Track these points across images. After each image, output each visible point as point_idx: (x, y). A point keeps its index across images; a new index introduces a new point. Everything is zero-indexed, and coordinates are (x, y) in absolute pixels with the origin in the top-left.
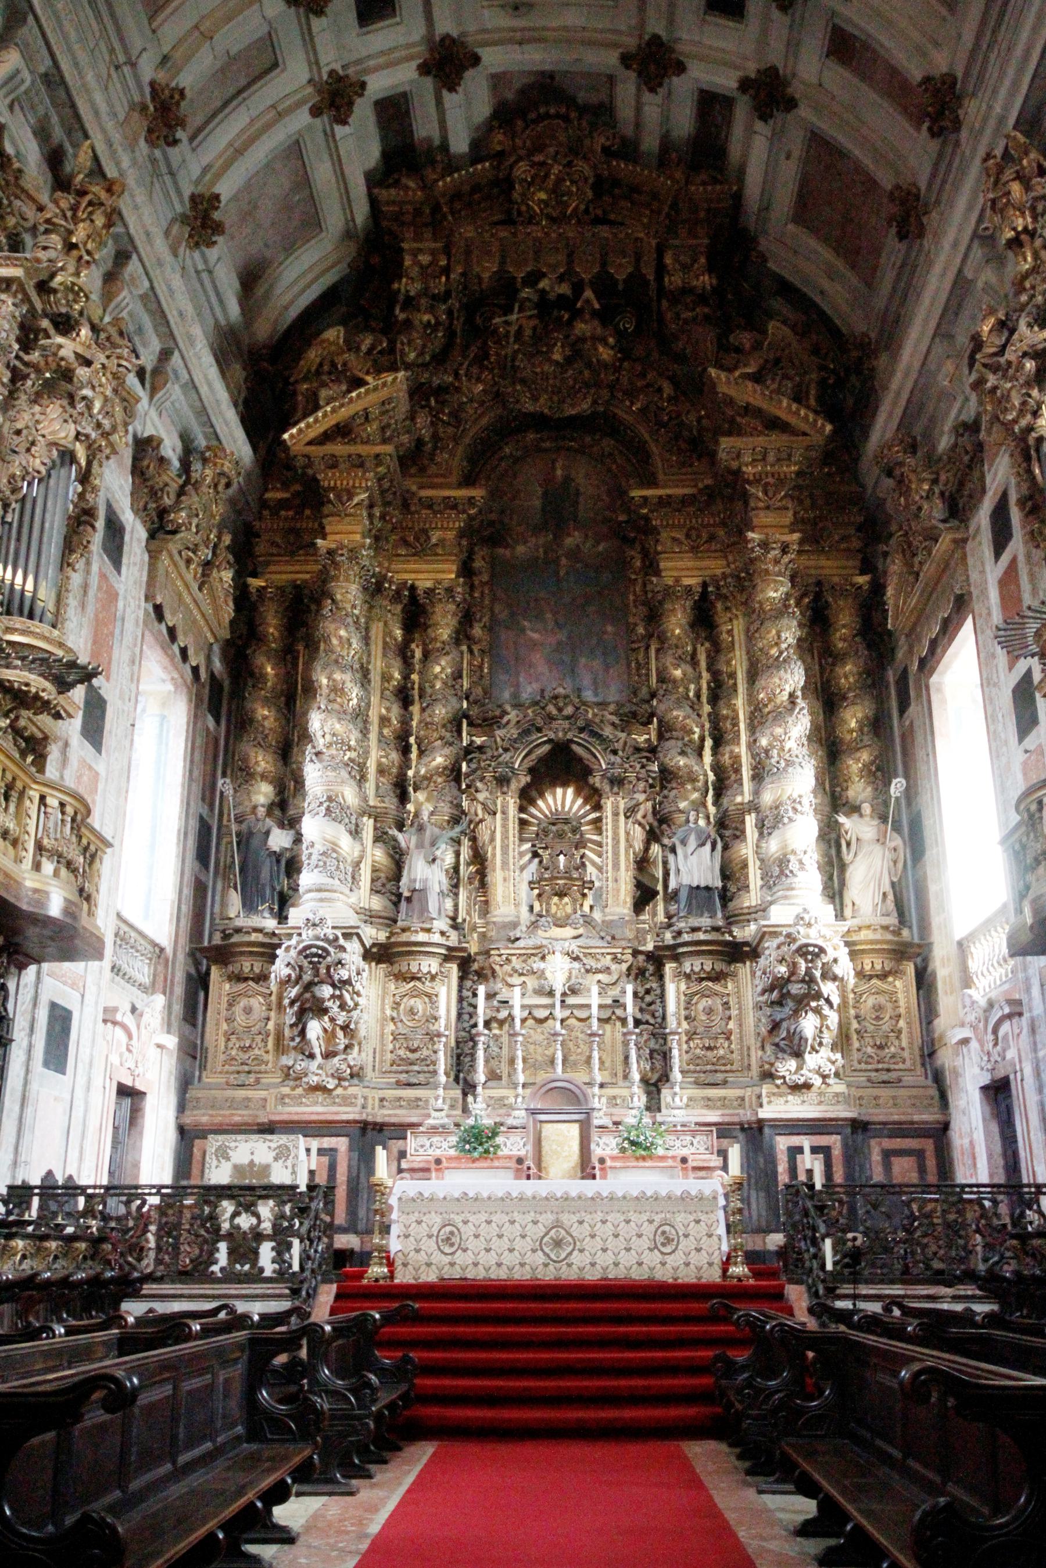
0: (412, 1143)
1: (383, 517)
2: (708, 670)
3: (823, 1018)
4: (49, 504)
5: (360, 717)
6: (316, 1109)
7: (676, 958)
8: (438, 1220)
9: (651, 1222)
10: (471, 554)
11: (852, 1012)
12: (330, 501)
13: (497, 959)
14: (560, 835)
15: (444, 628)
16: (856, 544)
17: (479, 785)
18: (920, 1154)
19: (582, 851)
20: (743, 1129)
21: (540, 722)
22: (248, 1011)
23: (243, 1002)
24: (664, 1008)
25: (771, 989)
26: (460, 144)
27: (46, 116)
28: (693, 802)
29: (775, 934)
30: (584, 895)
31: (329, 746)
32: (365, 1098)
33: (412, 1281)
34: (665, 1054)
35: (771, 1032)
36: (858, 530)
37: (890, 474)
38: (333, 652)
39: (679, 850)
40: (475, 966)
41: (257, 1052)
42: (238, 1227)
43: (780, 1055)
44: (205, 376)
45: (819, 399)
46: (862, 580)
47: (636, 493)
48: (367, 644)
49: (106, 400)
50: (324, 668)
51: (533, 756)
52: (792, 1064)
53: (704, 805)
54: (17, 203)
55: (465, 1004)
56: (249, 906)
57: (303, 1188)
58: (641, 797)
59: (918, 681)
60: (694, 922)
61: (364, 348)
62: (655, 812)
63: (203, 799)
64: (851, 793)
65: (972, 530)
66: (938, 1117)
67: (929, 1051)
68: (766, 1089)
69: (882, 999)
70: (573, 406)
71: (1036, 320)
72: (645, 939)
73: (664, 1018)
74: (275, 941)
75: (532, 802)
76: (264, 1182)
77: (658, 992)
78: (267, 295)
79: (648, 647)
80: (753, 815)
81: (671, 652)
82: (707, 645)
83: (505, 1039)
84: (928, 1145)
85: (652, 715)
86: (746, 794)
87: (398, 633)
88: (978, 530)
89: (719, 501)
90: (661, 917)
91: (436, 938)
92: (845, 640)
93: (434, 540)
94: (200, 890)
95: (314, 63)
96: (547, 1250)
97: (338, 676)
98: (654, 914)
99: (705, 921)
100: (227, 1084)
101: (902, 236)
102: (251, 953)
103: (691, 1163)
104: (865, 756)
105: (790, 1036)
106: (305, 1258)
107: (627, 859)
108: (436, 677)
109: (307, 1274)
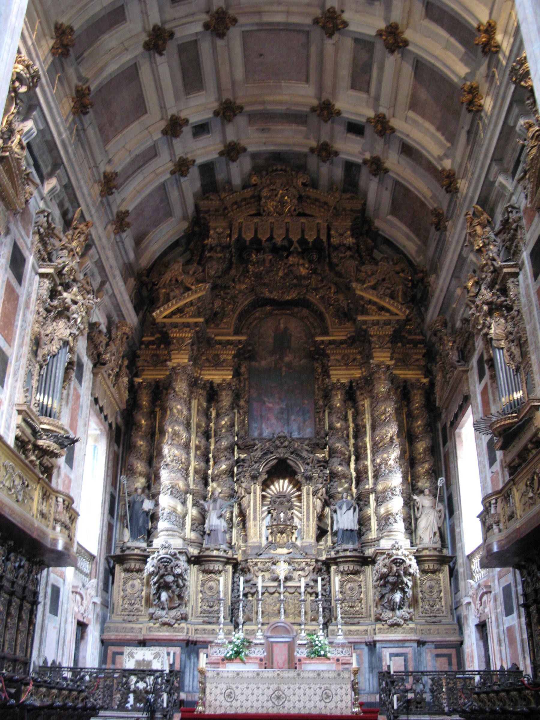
0: (211, 650)
1: (198, 348)
2: (353, 422)
3: (405, 593)
4: (58, 365)
5: (186, 447)
6: (165, 634)
7: (336, 564)
8: (224, 686)
9: (320, 688)
10: (239, 367)
11: (419, 589)
12: (173, 343)
13: (251, 564)
14: (282, 503)
15: (226, 400)
16: (422, 363)
17: (243, 479)
18: (449, 656)
19: (292, 511)
20: (367, 645)
21: (272, 449)
22: (133, 586)
23: (131, 582)
24: (330, 587)
25: (380, 579)
26: (237, 181)
27: (63, 199)
28: (345, 489)
29: (383, 554)
30: (293, 533)
31: (172, 461)
32: (188, 629)
33: (213, 713)
34: (330, 610)
35: (380, 599)
36: (424, 356)
37: (435, 335)
38: (175, 416)
39: (338, 511)
40: (240, 567)
41: (137, 606)
42: (138, 688)
43: (384, 610)
44: (120, 291)
45: (405, 294)
46: (425, 381)
47: (319, 339)
48: (190, 411)
49: (83, 317)
50: (169, 425)
51: (269, 465)
52: (390, 614)
53: (350, 489)
54: (52, 240)
55: (235, 585)
56: (134, 536)
57: (167, 671)
58: (321, 486)
59: (451, 432)
60: (345, 546)
61: (191, 272)
62: (327, 492)
63: (112, 484)
64: (420, 484)
65: (470, 366)
66: (458, 638)
67: (455, 607)
68: (379, 626)
69: (433, 583)
70: (288, 295)
71: (489, 287)
72: (322, 554)
73: (330, 592)
74: (146, 553)
75: (268, 487)
76: (149, 668)
77: (328, 579)
78: (146, 248)
79: (324, 411)
80: (374, 495)
81: (335, 415)
82: (353, 410)
83: (255, 602)
84: (453, 651)
85: (326, 445)
86: (370, 485)
87: (205, 404)
88: (472, 367)
89: (358, 342)
90: (330, 543)
91: (222, 554)
92: (418, 409)
93: (222, 360)
94: (110, 527)
95: (172, 153)
96: (274, 700)
97: (176, 428)
98: (326, 541)
99: (350, 546)
100: (124, 620)
101: (437, 229)
102: (135, 559)
103: (340, 662)
104: (426, 466)
105: (389, 601)
106: (169, 702)
107: (313, 516)
108: (223, 426)
109: (169, 708)
